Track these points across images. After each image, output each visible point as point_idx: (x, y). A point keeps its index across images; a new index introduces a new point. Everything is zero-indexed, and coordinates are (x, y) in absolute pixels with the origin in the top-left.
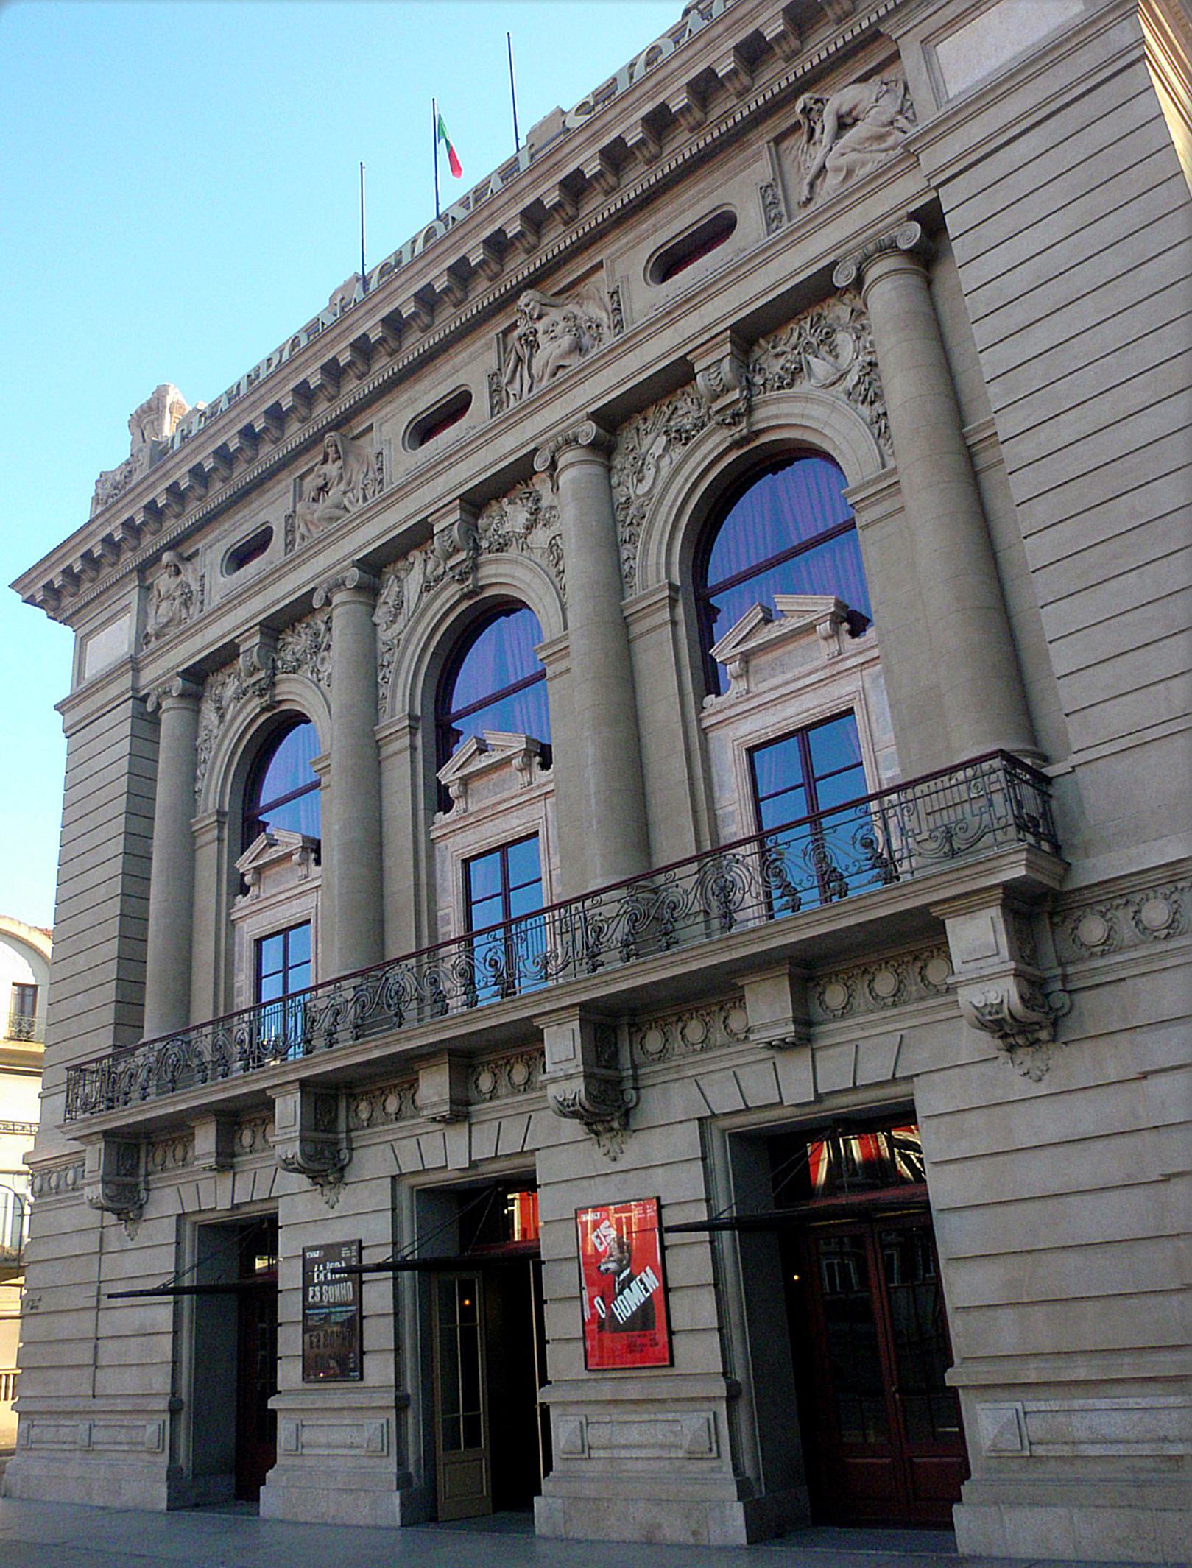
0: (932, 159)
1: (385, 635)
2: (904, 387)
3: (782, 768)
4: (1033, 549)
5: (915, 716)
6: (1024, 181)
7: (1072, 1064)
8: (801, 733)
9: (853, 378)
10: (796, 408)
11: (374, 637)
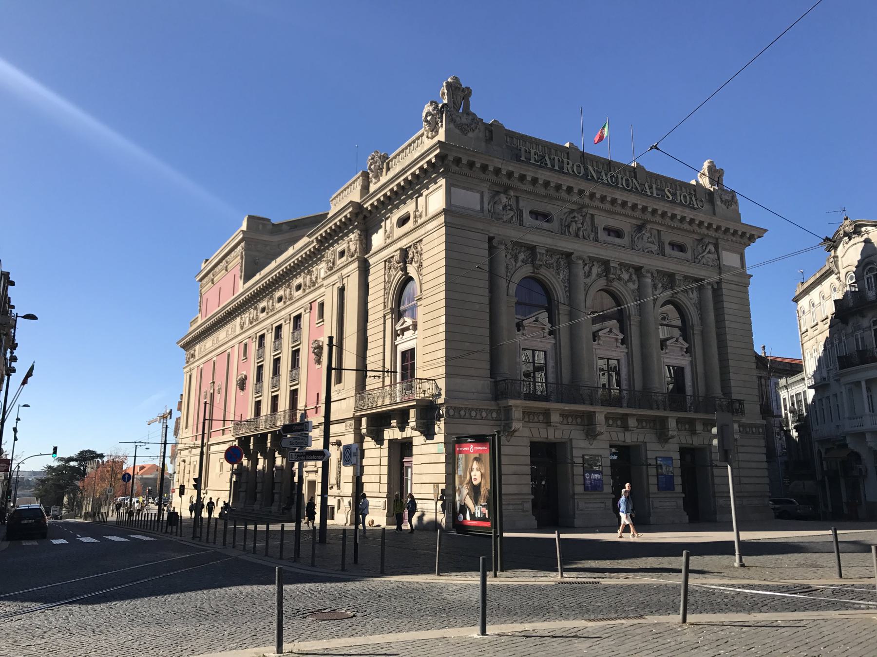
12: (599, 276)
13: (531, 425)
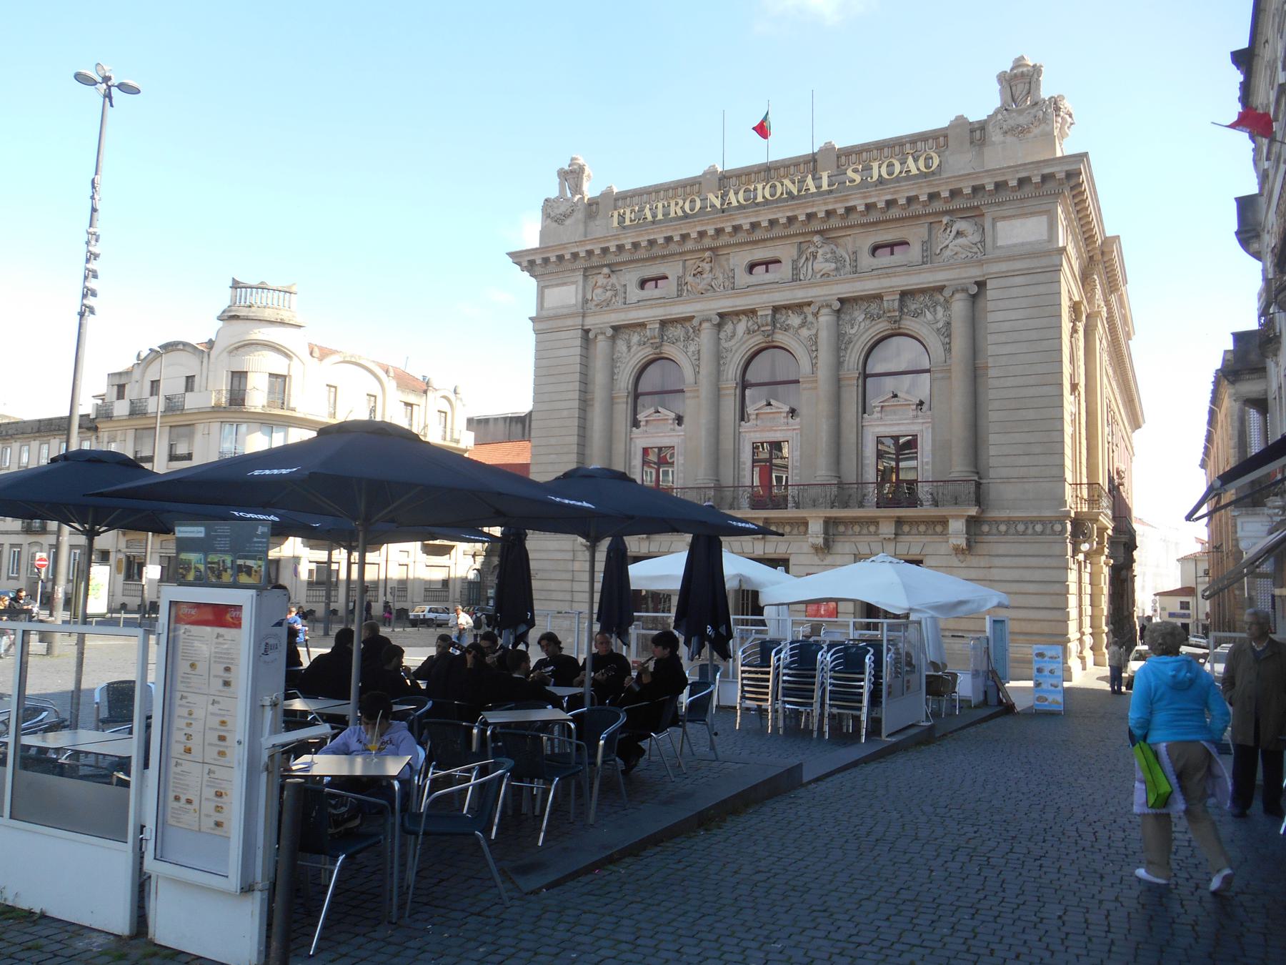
1: (724, 344)
4: (993, 416)
5: (941, 447)
6: (1015, 292)
7: (973, 561)
9: (940, 325)
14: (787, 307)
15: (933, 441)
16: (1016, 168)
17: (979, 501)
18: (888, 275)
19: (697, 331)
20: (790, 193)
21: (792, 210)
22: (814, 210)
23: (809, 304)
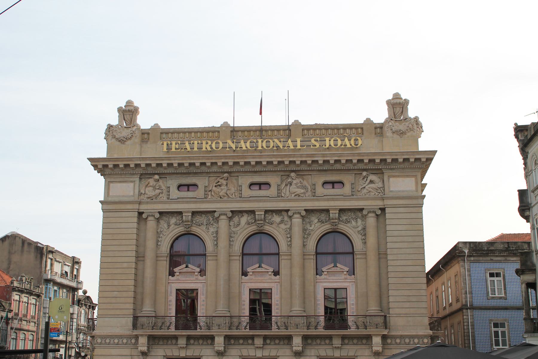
0: (388, 202)
2: (372, 240)
3: (331, 294)
8: (336, 289)
9: (360, 229)
10: (347, 228)
11: (230, 229)
12: (248, 223)
13: (165, 347)
14: (272, 211)
15: (357, 292)
16: (402, 153)
17: (386, 325)
18: (333, 200)
19: (217, 220)
20: (278, 147)
21: (282, 158)
22: (294, 159)
23: (287, 211)
